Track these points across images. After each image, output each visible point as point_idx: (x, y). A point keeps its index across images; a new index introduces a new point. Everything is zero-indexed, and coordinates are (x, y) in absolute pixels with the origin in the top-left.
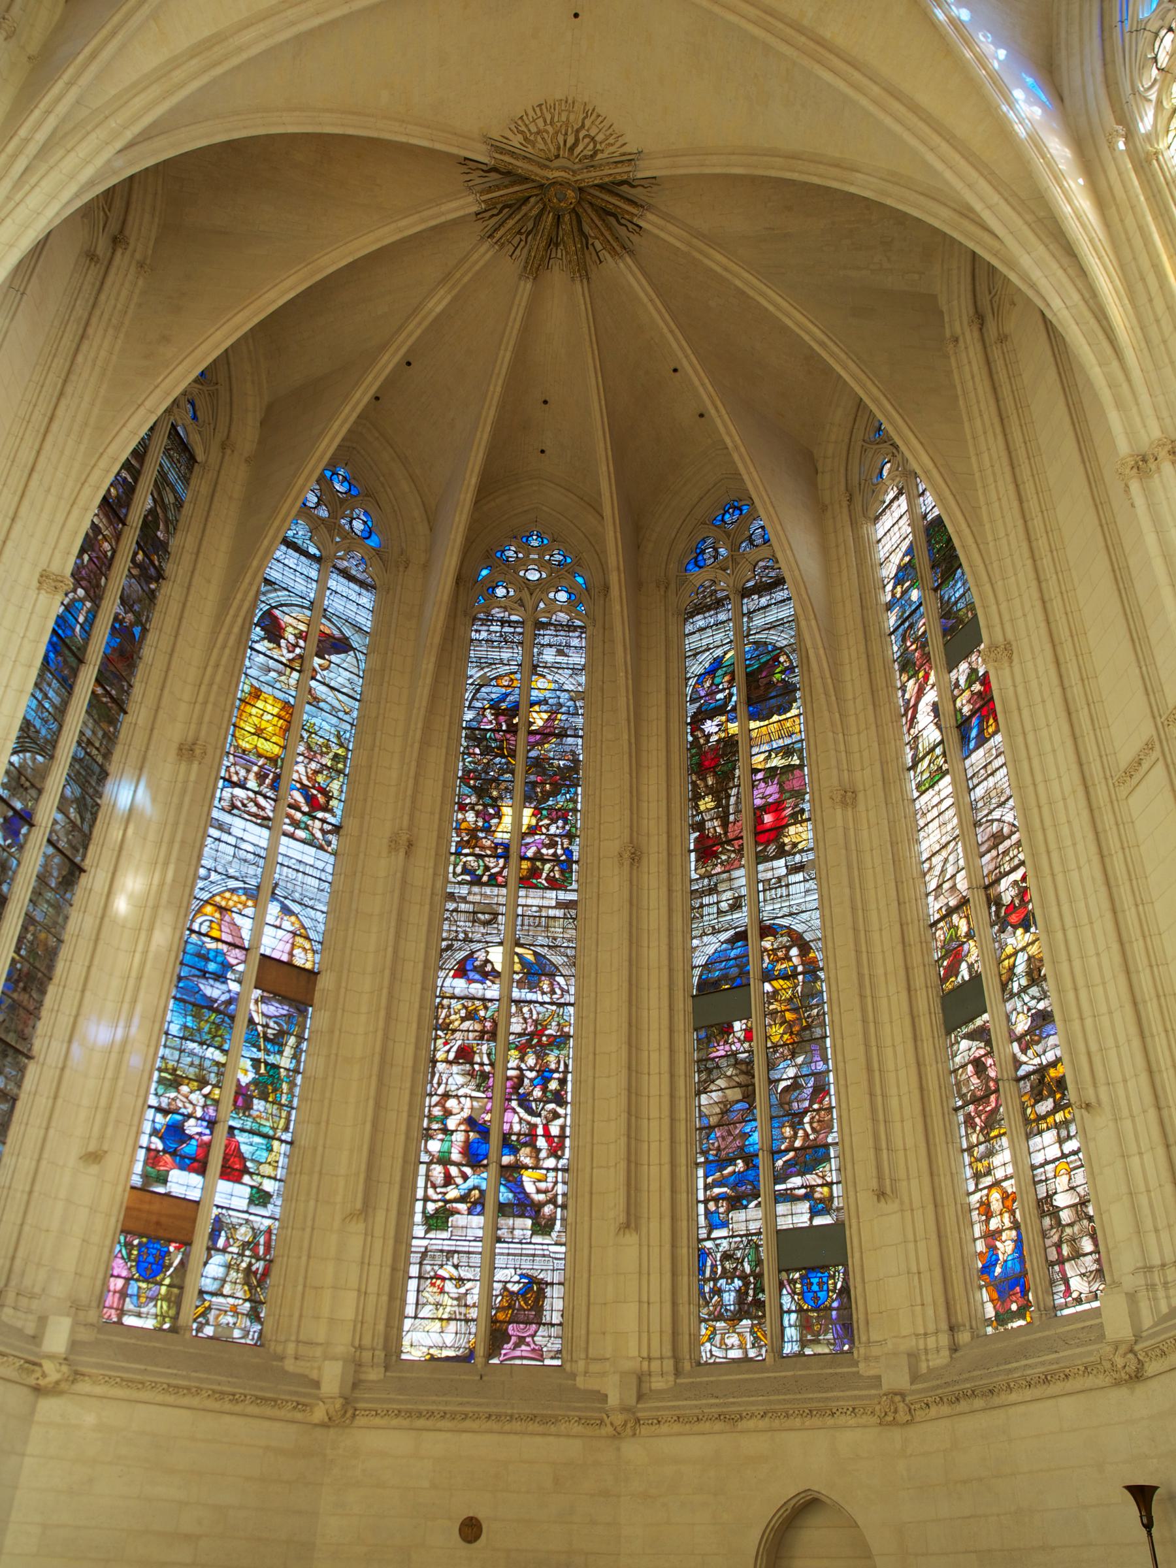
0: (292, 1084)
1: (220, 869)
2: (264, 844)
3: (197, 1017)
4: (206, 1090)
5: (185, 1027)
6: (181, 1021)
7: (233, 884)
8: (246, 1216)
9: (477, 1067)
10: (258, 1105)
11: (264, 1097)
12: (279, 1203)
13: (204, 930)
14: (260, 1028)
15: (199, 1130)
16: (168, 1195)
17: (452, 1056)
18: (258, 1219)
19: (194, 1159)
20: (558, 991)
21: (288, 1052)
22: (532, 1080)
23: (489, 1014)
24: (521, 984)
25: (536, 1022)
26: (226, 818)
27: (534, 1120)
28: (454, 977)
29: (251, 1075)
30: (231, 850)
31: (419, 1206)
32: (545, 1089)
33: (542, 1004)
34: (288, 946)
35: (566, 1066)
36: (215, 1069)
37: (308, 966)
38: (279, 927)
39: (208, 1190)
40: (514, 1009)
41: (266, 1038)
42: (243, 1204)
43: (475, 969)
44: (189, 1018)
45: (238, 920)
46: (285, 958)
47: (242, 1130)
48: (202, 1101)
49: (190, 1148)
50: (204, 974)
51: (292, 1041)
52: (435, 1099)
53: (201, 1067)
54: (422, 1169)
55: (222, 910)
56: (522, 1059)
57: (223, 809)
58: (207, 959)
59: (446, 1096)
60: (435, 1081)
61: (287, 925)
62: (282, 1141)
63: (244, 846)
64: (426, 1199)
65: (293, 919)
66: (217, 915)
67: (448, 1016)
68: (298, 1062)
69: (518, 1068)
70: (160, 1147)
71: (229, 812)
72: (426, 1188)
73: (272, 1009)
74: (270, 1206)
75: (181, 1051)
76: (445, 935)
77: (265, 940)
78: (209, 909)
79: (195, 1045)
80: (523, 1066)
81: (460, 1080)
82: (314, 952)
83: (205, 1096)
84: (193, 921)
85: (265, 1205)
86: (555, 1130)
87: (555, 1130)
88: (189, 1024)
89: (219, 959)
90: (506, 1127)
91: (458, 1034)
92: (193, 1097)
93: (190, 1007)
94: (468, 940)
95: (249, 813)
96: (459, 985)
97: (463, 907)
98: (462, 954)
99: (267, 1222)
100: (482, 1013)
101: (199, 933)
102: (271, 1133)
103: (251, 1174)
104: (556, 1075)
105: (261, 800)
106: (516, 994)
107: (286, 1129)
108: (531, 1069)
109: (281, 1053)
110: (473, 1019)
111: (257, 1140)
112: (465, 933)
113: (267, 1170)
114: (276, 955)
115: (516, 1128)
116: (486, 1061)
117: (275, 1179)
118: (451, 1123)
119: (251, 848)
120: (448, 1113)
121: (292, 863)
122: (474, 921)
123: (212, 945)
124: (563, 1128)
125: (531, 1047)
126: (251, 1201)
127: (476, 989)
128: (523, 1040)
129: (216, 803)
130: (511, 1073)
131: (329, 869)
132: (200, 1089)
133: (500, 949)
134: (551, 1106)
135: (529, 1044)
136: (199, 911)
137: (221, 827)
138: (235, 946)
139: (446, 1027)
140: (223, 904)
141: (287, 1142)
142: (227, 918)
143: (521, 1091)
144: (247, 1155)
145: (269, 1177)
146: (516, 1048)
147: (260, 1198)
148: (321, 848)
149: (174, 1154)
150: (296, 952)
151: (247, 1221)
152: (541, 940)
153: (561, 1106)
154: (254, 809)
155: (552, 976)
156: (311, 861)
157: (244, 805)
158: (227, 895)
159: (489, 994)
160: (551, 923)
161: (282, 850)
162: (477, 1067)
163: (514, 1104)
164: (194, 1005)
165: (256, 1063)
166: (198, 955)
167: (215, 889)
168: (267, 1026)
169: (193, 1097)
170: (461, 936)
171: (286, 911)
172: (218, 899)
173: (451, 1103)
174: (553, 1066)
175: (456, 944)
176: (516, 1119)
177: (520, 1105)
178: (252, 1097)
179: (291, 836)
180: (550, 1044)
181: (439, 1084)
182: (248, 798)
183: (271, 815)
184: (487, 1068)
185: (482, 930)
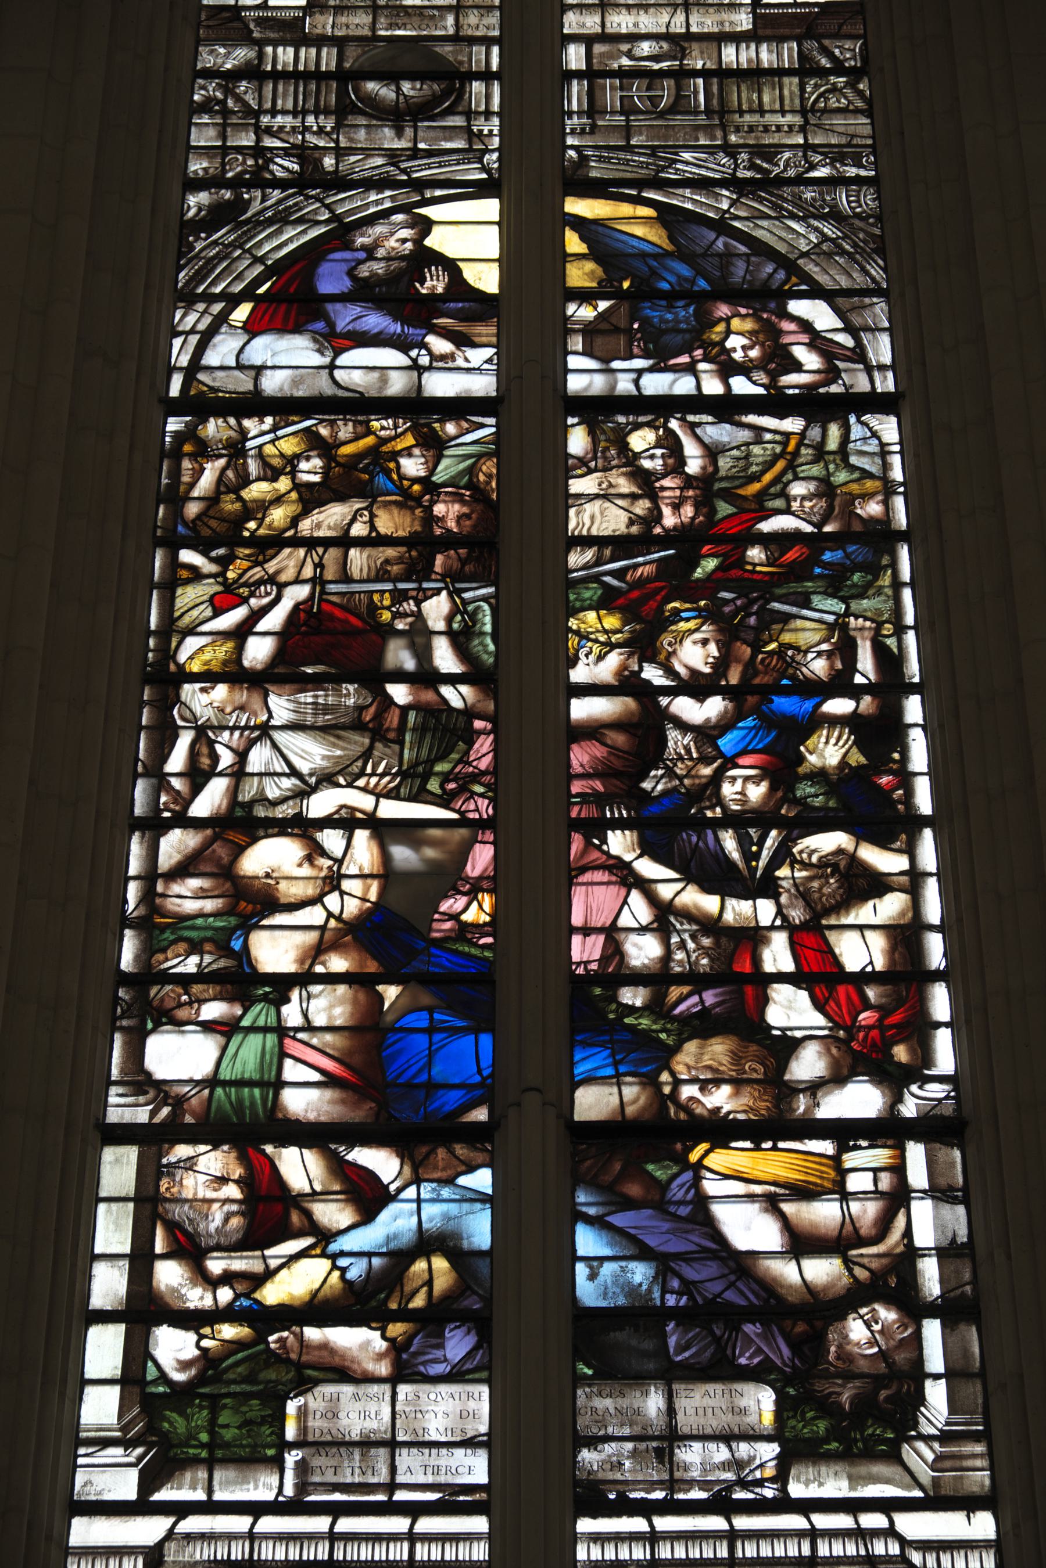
9: (399, 693)
17: (258, 651)
20: (810, 360)
22: (706, 734)
23: (446, 469)
24: (603, 342)
25: (705, 488)
27: (737, 910)
28: (252, 329)
31: (104, 1349)
32: (782, 767)
33: (727, 408)
35: (889, 661)
40: (578, 441)
43: (364, 292)
52: (174, 844)
54: (119, 1169)
56: (645, 644)
59: (242, 824)
60: (177, 761)
64: (144, 1311)
67: (232, 484)
69: (627, 684)
72: (140, 1261)
76: (197, 166)
80: (653, 674)
81: (310, 753)
86: (858, 951)
87: (858, 951)
90: (584, 950)
91: (287, 562)
94: (312, 179)
96: (287, 359)
97: (286, 55)
98: (292, 239)
100: (413, 466)
104: (839, 706)
106: (583, 377)
108: (697, 687)
110: (369, 493)
112: (302, 153)
115: (643, 951)
116: (445, 659)
118: (274, 951)
120: (256, 903)
122: (343, 112)
124: (905, 936)
125: (690, 591)
127: (367, 367)
128: (645, 565)
130: (582, 709)
133: (490, 208)
134: (828, 842)
135: (675, 579)
139: (227, 531)
143: (654, 783)
146: (607, 601)
152: (689, 162)
153: (883, 843)
155: (766, 301)
159: (441, 385)
160: (740, 95)
162: (399, 693)
163: (619, 843)
170: (284, 166)
173: (271, 857)
174: (819, 667)
175: (256, 202)
176: (638, 910)
177: (648, 849)
180: (798, 572)
181: (198, 776)
184: (454, 696)
185: (388, 138)
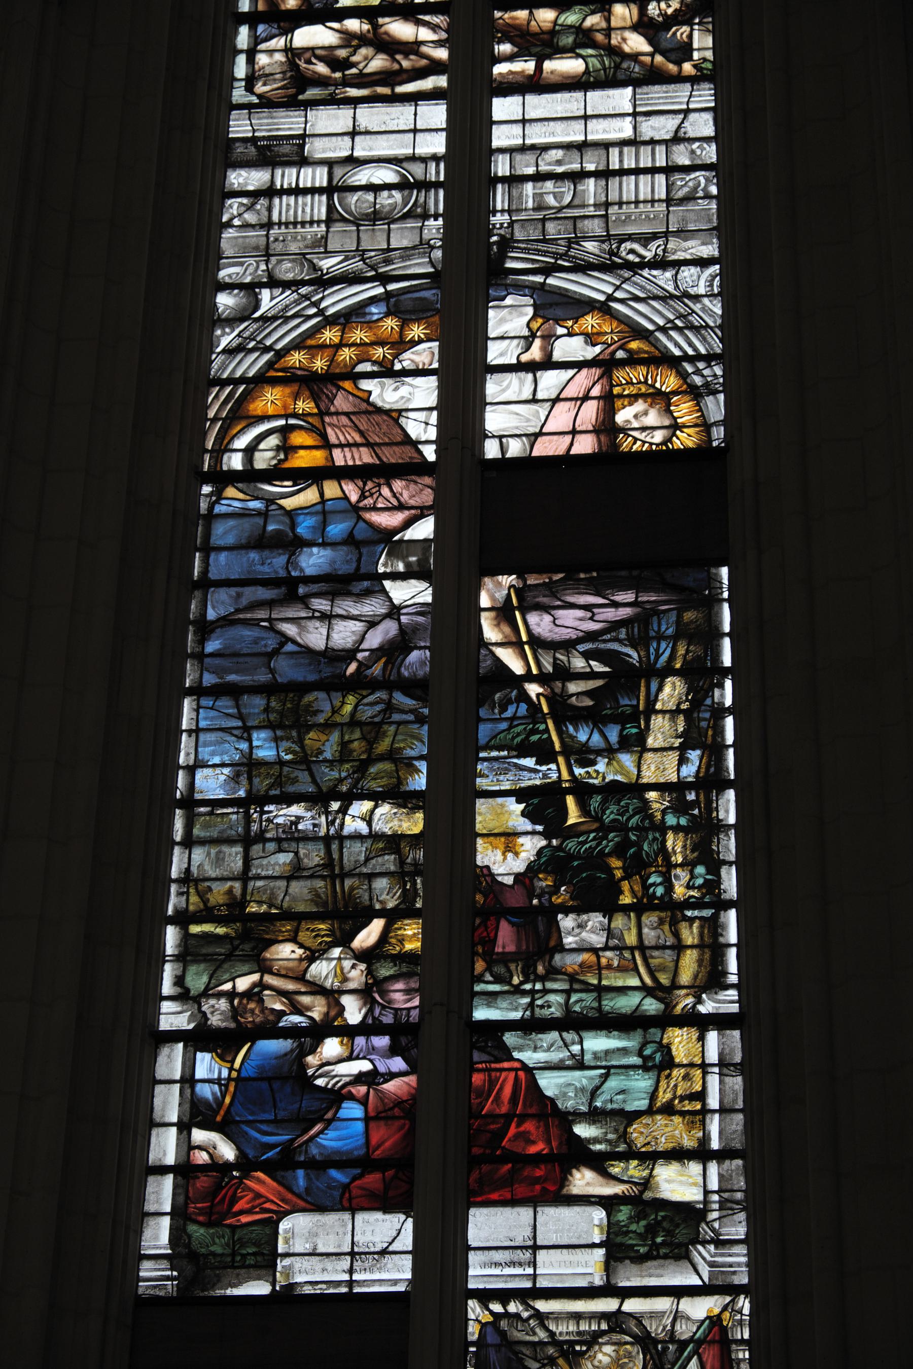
0: (705, 829)
1: (287, 270)
2: (437, 144)
3: (291, 721)
4: (368, 936)
5: (248, 766)
6: (234, 749)
7: (337, 300)
8: (609, 1305)
10: (581, 931)
11: (598, 897)
12: (738, 1230)
13: (263, 460)
14: (533, 689)
15: (364, 1066)
16: (287, 1297)
18: (663, 1304)
19: (361, 1162)
21: (661, 732)
26: (288, 123)
29: (530, 846)
30: (319, 207)
34: (590, 411)
36: (389, 862)
37: (686, 439)
38: (548, 363)
39: (442, 1252)
41: (563, 711)
42: (589, 1267)
44: (259, 738)
45: (385, 394)
46: (585, 445)
47: (532, 1026)
48: (357, 975)
49: (347, 1130)
50: (291, 590)
51: (672, 692)
53: (332, 870)
55: (314, 384)
57: (267, 103)
58: (294, 544)
61: (570, 348)
62: (702, 1024)
63: (363, 176)
65: (590, 322)
66: (304, 405)
68: (715, 751)
70: (228, 1152)
71: (292, 103)
73: (569, 617)
74: (703, 1254)
75: (248, 841)
77: (495, 420)
78: (271, 399)
79: (296, 810)
82: (696, 394)
83: (366, 956)
84: (223, 448)
85: (680, 1254)
88: (266, 752)
89: (336, 529)
92: (321, 970)
93: (257, 702)
95: (363, 80)
99: (699, 1308)
101: (250, 476)
102: (652, 1006)
103: (598, 1163)
105: (401, 29)
107: (713, 980)
109: (636, 744)
111: (597, 1043)
113: (670, 1132)
114: (545, 448)
117: (702, 1154)
119: (387, 175)
121: (549, 162)
123: (310, 496)
126: (616, 1250)
129: (239, 94)
131: (703, 125)
132: (345, 940)
136: (239, 416)
137: (268, 153)
138: (384, 472)
140: (319, 364)
141: (721, 1022)
142: (341, 402)
144: (568, 1104)
145: (678, 1155)
147: (650, 1231)
148: (655, 77)
149: (282, 1164)
150: (623, 416)
151: (616, 1320)
154: (378, 63)
156: (624, 128)
157: (346, 64)
158: (330, 335)
161: (501, 137)
164: (268, 690)
165: (542, 804)
166: (261, 542)
167: (281, 336)
168: (564, 674)
169: (321, 970)
171: (555, 308)
172: (296, 358)
178: (551, 913)
179: (535, 85)
182: (351, 40)
183: (442, 54)
